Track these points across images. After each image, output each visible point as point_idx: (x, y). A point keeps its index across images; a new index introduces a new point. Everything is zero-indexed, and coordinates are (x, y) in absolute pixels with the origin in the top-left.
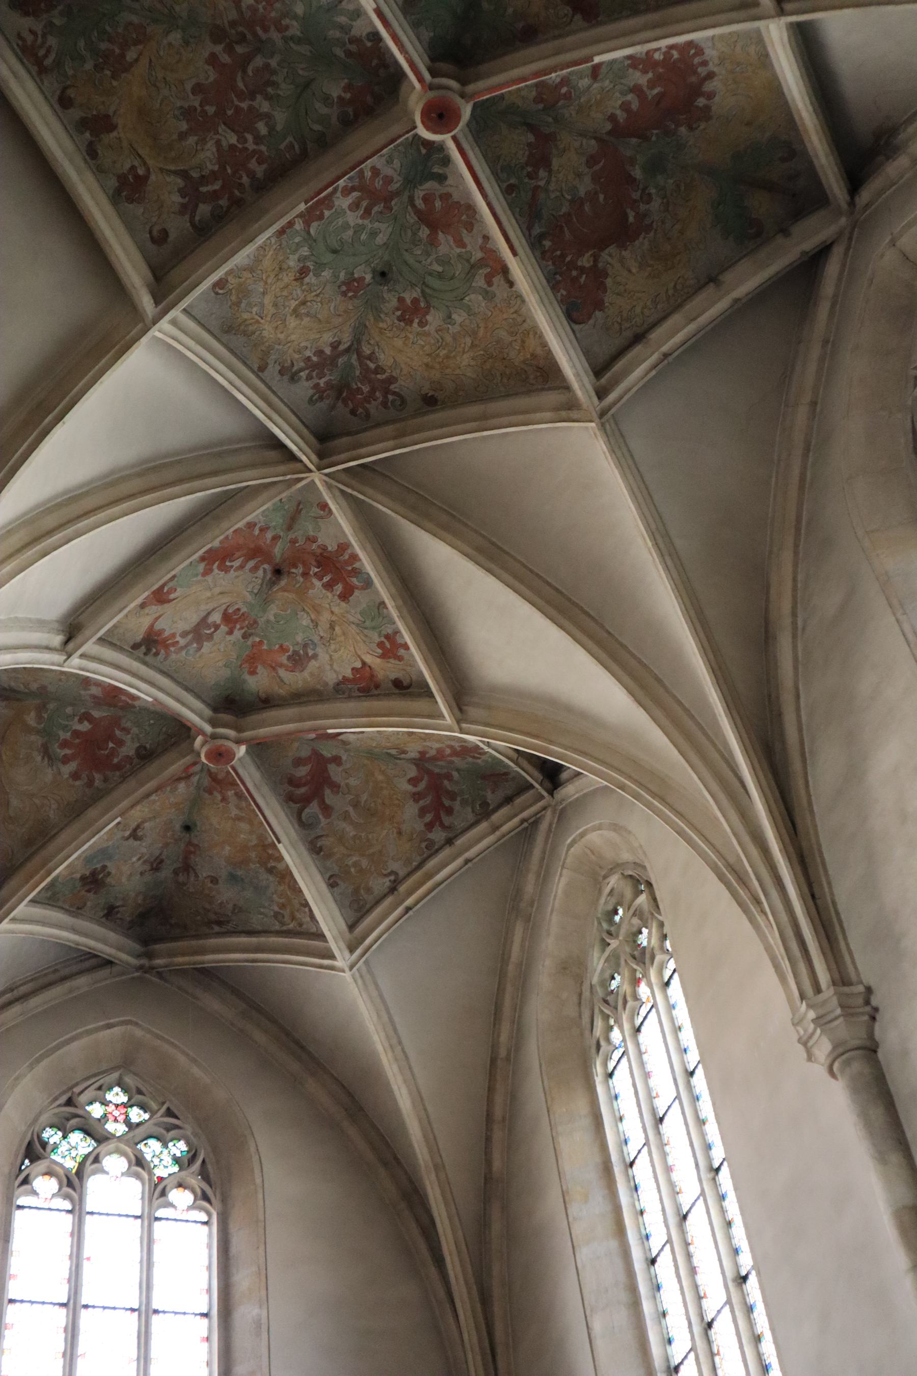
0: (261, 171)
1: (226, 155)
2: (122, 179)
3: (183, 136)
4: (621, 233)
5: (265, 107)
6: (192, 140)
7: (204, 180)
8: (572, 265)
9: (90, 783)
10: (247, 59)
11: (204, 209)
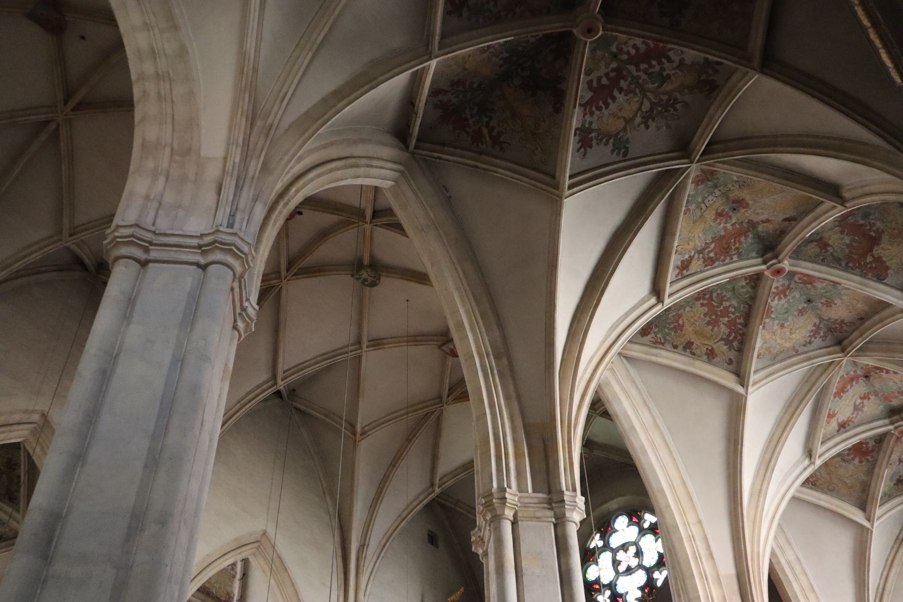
0: (741, 321)
1: (729, 325)
2: (706, 354)
3: (712, 330)
4: (874, 241)
5: (728, 304)
6: (716, 329)
7: (728, 336)
8: (866, 264)
9: (868, 461)
10: (711, 298)
11: (735, 344)
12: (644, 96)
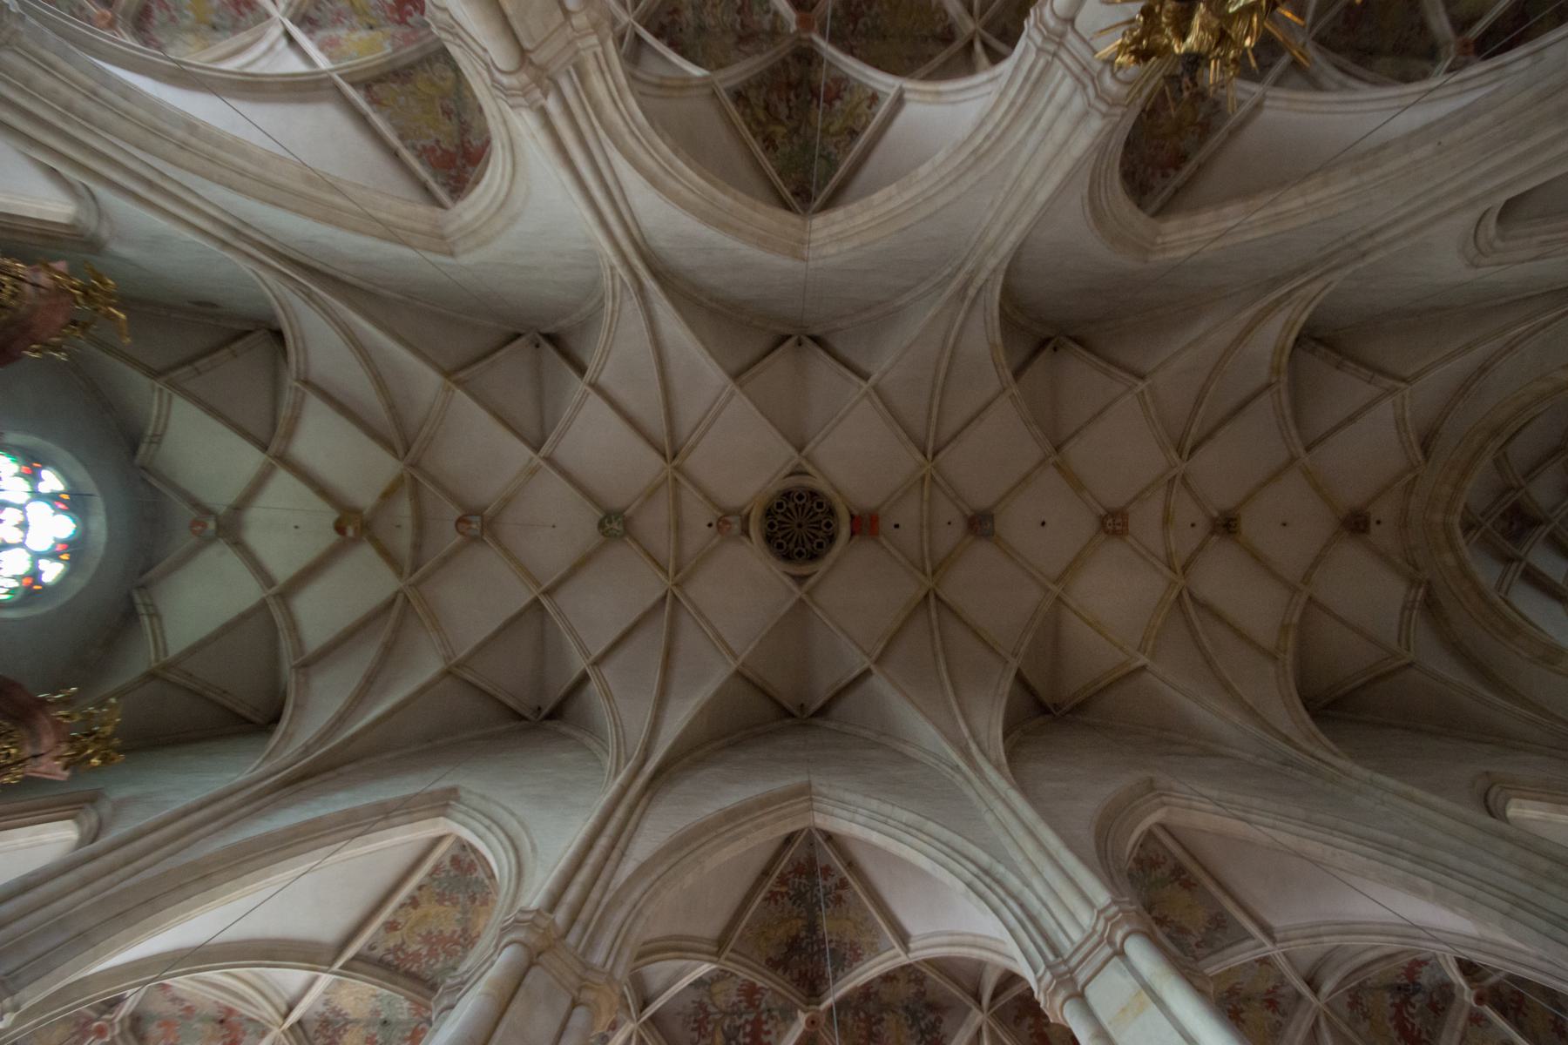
0: (414, 969)
1: (416, 956)
10: (457, 943)
11: (390, 957)
12: (721, 1012)
